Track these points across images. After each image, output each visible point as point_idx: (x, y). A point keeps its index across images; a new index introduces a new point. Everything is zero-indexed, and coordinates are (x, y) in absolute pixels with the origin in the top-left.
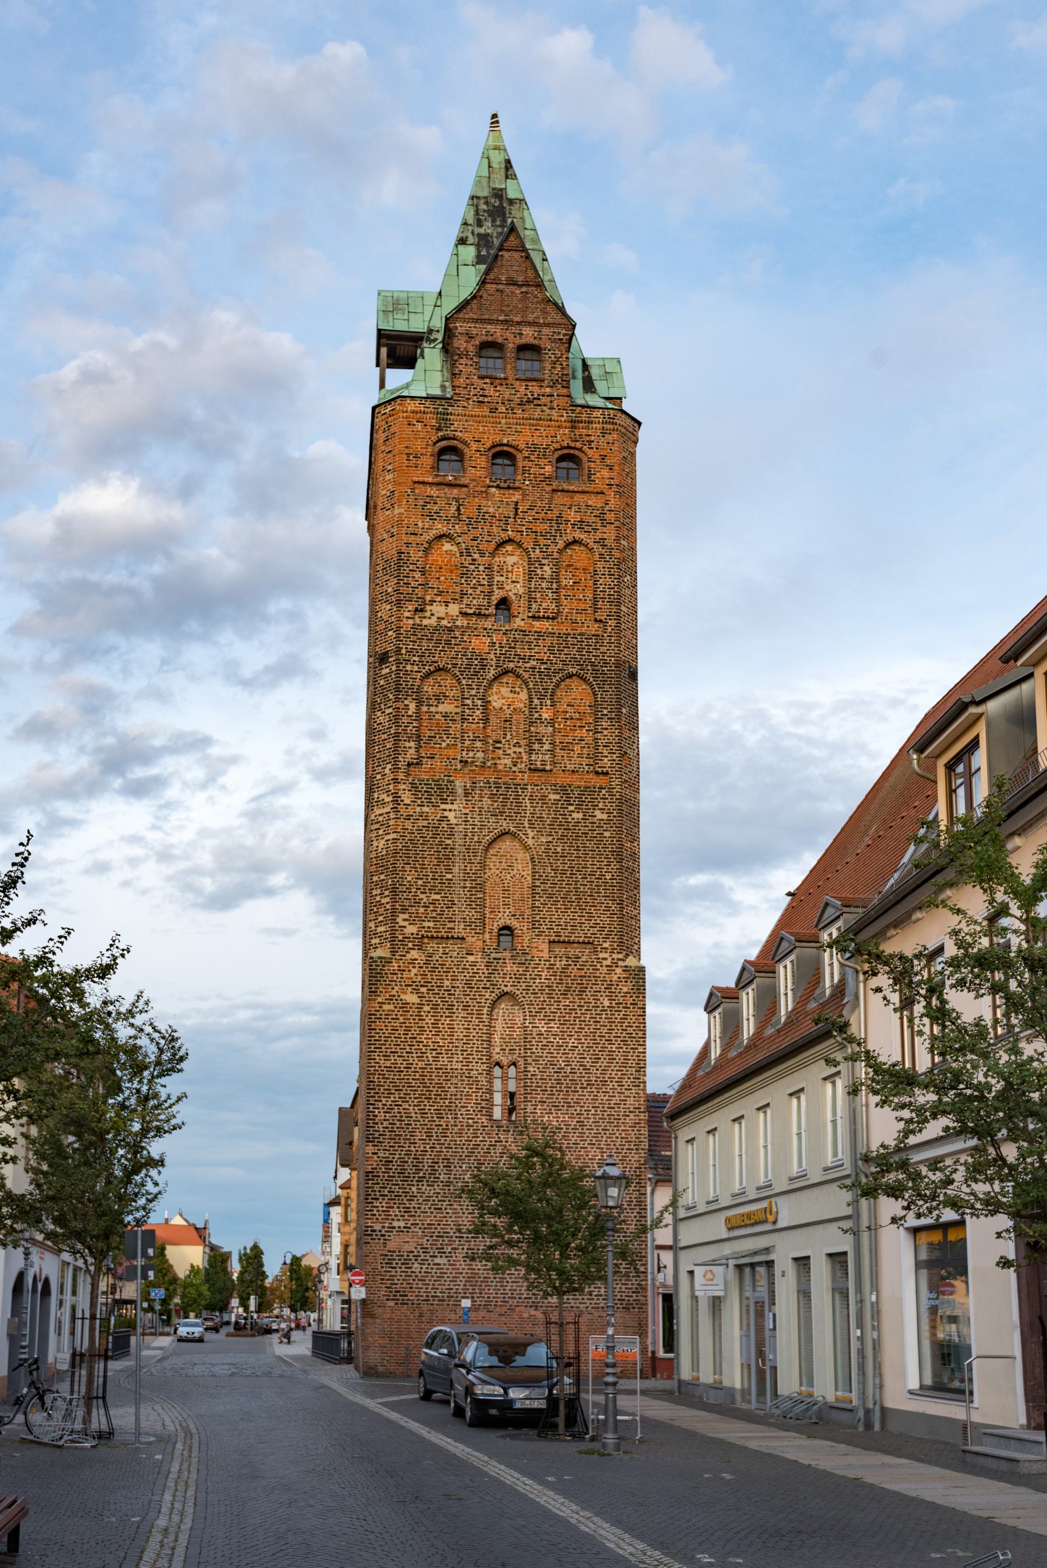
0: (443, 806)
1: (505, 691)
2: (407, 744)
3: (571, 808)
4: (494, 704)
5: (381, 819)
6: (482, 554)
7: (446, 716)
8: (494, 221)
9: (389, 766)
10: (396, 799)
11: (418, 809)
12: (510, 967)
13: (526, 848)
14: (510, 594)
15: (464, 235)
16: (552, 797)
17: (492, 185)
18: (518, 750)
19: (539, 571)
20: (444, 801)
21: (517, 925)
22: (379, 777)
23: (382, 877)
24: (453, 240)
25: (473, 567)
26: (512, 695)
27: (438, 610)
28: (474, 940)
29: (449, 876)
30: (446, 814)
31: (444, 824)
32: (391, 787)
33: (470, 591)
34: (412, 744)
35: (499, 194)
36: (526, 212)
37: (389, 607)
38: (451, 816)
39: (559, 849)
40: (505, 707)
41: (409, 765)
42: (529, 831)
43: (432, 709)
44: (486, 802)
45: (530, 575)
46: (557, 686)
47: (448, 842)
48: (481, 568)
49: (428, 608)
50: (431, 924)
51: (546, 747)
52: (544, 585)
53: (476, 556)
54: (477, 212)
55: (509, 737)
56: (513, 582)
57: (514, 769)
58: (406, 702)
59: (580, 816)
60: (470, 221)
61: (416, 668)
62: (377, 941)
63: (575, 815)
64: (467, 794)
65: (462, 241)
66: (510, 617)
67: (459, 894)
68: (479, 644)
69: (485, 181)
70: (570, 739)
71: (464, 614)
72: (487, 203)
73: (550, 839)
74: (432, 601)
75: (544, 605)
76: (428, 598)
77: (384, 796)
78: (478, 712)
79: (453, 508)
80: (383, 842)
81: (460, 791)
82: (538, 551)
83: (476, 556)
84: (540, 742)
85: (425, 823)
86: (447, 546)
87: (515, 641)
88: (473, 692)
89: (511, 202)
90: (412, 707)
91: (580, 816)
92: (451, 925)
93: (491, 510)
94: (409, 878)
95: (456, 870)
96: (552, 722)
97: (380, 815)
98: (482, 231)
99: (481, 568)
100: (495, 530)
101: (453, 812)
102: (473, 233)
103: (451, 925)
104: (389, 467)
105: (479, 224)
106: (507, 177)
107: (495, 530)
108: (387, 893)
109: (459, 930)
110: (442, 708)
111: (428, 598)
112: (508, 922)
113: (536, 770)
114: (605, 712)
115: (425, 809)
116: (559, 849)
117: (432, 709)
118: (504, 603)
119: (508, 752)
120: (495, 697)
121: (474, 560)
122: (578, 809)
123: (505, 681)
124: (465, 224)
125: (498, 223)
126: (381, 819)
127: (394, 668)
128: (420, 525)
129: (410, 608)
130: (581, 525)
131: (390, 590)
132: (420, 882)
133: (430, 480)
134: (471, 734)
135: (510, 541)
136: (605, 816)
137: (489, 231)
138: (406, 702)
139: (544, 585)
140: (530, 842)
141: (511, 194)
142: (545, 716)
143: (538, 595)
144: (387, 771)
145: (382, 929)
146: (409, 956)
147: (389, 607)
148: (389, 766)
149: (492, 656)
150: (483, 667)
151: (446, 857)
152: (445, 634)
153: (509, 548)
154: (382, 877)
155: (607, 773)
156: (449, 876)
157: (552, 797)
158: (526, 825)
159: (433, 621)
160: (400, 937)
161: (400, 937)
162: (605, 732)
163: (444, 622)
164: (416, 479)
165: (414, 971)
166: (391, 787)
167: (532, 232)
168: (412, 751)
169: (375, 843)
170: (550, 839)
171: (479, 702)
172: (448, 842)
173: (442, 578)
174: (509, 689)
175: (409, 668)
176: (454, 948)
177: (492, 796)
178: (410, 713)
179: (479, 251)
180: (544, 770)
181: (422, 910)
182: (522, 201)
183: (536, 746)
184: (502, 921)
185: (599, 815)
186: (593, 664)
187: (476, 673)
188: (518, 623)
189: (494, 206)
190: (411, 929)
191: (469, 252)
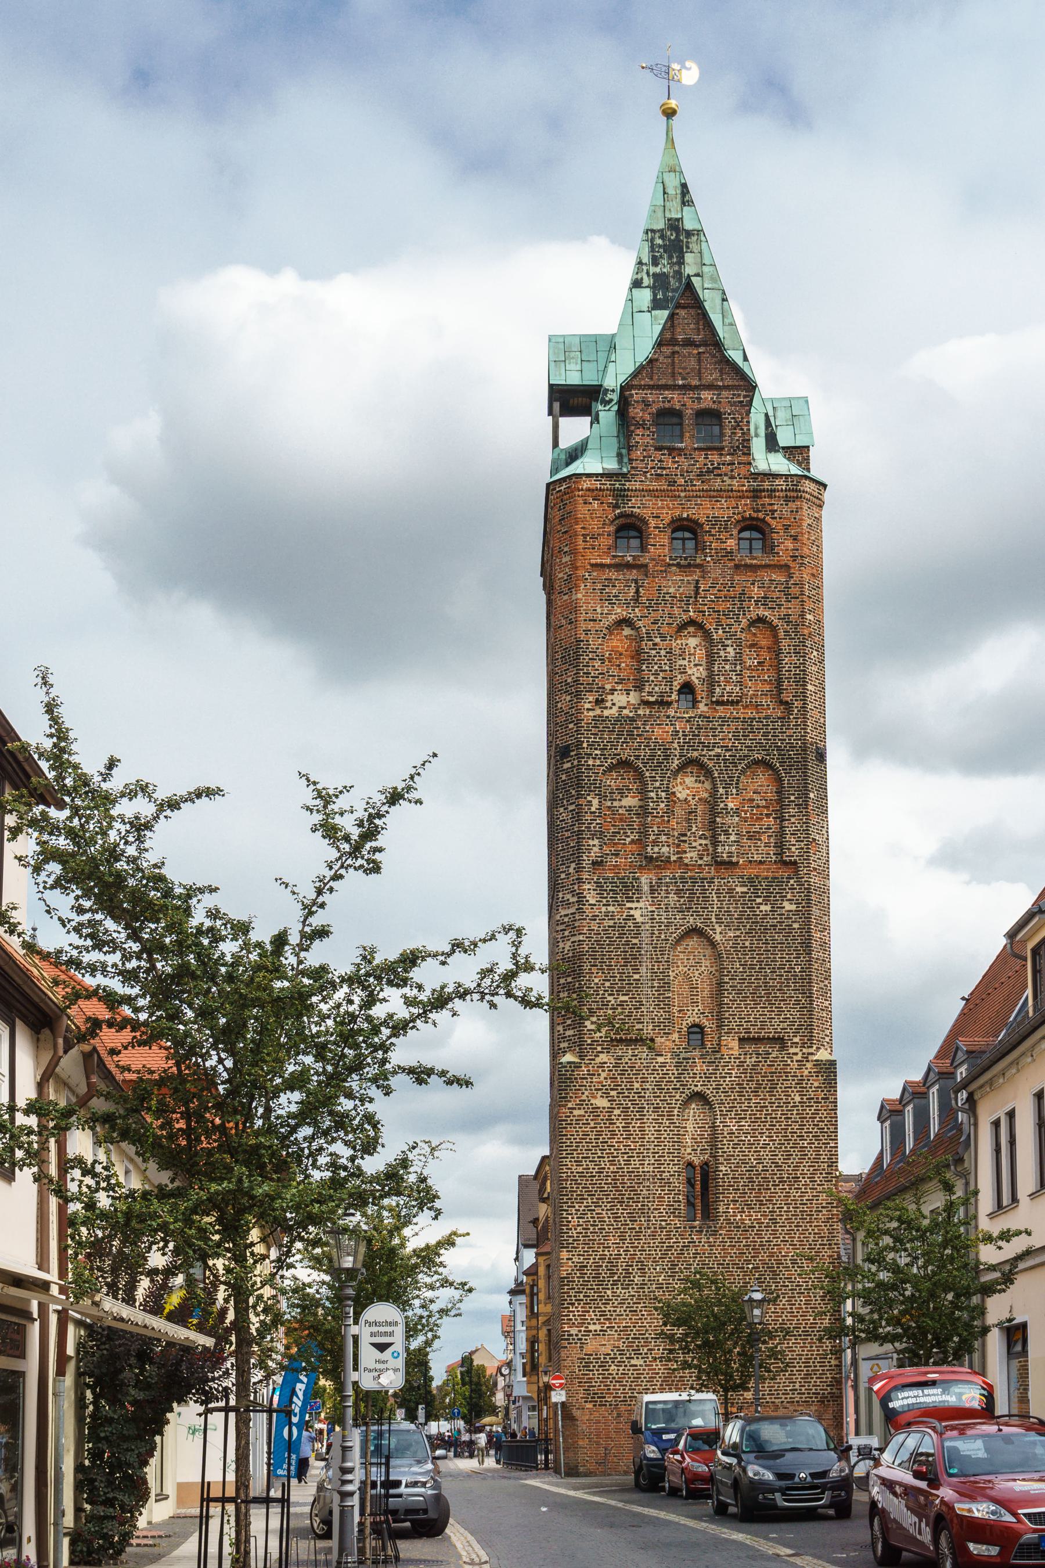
0: (629, 905)
1: (689, 781)
2: (591, 842)
3: (759, 900)
4: (678, 795)
5: (566, 919)
6: (663, 638)
7: (629, 809)
8: (670, 257)
9: (573, 865)
10: (581, 899)
11: (604, 909)
12: (700, 1067)
13: (713, 944)
14: (693, 678)
15: (639, 276)
16: (739, 889)
17: (668, 215)
18: (704, 842)
19: (722, 653)
20: (630, 900)
21: (707, 1023)
22: (563, 876)
23: (569, 979)
24: (627, 283)
25: (654, 652)
26: (697, 785)
27: (620, 699)
28: (663, 1040)
29: (636, 977)
30: (632, 912)
32: (576, 887)
33: (652, 678)
34: (596, 842)
35: (675, 225)
36: (704, 244)
37: (568, 698)
38: (637, 914)
39: (747, 944)
40: (690, 798)
41: (594, 863)
42: (716, 926)
43: (615, 804)
45: (711, 658)
46: (743, 772)
47: (635, 941)
48: (663, 653)
49: (610, 697)
51: (733, 838)
52: (727, 667)
53: (658, 640)
54: (652, 248)
55: (694, 829)
56: (696, 665)
57: (700, 862)
58: (589, 798)
59: (768, 908)
60: (645, 260)
61: (598, 762)
62: (566, 1045)
63: (763, 908)
64: (652, 891)
65: (637, 284)
66: (695, 703)
67: (648, 993)
68: (660, 733)
69: (660, 214)
71: (647, 703)
72: (662, 237)
73: (738, 933)
74: (613, 691)
75: (728, 688)
76: (608, 687)
77: (569, 896)
78: (662, 805)
79: (633, 590)
80: (569, 943)
81: (646, 888)
82: (720, 632)
83: (658, 640)
84: (727, 833)
85: (611, 923)
86: (627, 631)
87: (699, 728)
88: (657, 784)
89: (689, 234)
90: (595, 802)
91: (768, 908)
92: (640, 1026)
93: (672, 590)
94: (596, 980)
96: (737, 812)
97: (566, 915)
98: (657, 270)
99: (663, 653)
100: (676, 611)
101: (639, 910)
102: (648, 273)
103: (640, 1026)
104: (566, 549)
105: (655, 262)
106: (683, 203)
107: (676, 611)
108: (574, 996)
109: (648, 1030)
111: (608, 687)
112: (697, 1020)
113: (723, 863)
114: (792, 798)
115: (611, 908)
116: (747, 944)
117: (615, 804)
118: (687, 688)
119: (694, 844)
120: (680, 788)
121: (655, 644)
122: (766, 901)
123: (689, 770)
124: (640, 263)
125: (675, 260)
126: (566, 919)
127: (576, 763)
128: (599, 610)
129: (591, 699)
130: (764, 601)
131: (569, 680)
132: (607, 984)
133: (608, 561)
134: (655, 829)
135: (692, 622)
136: (793, 907)
137: (665, 270)
138: (589, 798)
139: (727, 667)
140: (718, 937)
141: (689, 225)
142: (731, 805)
143: (722, 678)
144: (571, 870)
145: (569, 1033)
146: (598, 1060)
147: (568, 698)
148: (573, 865)
149: (676, 745)
150: (667, 757)
151: (633, 958)
152: (625, 725)
153: (691, 629)
154: (569, 979)
155: (795, 863)
156: (636, 977)
157: (739, 889)
158: (714, 920)
159: (614, 711)
160: (589, 1041)
161: (589, 1041)
162: (793, 820)
163: (626, 712)
164: (593, 561)
165: (603, 1075)
166: (576, 887)
167: (712, 268)
168: (596, 849)
169: (561, 945)
170: (738, 933)
171: (663, 794)
172: (635, 941)
173: (623, 665)
174: (693, 779)
175: (590, 762)
176: (643, 1052)
177: (678, 892)
178: (593, 809)
179: (655, 295)
180: (730, 863)
181: (610, 1012)
182: (699, 232)
183: (722, 838)
184: (691, 1019)
185: (788, 906)
186: (779, 749)
188: (702, 707)
189: (670, 239)
191: (645, 296)
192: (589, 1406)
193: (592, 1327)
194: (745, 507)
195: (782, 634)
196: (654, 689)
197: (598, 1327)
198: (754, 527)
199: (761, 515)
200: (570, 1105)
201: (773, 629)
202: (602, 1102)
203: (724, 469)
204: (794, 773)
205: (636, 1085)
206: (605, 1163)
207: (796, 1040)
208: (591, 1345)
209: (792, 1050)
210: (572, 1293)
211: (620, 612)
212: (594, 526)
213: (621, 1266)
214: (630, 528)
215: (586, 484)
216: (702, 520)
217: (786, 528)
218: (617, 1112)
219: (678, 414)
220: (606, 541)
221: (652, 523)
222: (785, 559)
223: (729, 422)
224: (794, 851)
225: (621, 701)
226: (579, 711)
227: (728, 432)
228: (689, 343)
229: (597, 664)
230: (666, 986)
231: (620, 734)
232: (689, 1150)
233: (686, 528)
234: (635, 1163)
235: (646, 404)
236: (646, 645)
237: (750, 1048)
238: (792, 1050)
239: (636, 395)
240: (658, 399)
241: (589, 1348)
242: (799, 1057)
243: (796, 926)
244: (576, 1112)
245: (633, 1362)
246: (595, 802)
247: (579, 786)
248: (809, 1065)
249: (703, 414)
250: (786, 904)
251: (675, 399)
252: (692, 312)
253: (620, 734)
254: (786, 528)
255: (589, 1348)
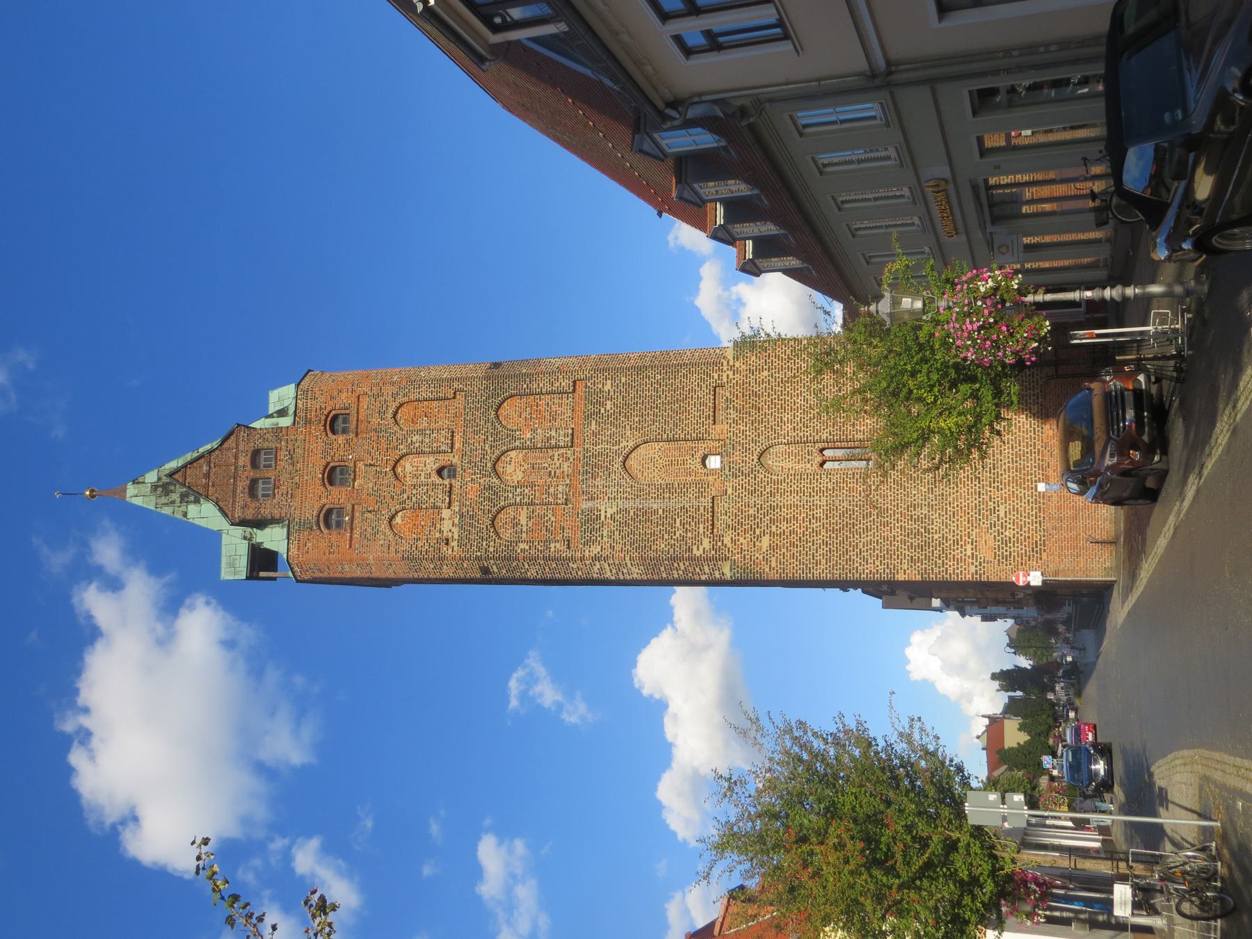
1: (510, 469)
3: (603, 410)
6: (404, 491)
7: (530, 518)
10: (596, 558)
20: (599, 517)
27: (446, 526)
29: (660, 512)
31: (617, 517)
38: (610, 511)
44: (598, 482)
45: (420, 453)
50: (701, 526)
51: (553, 433)
59: (609, 403)
62: (717, 573)
63: (608, 407)
64: (592, 499)
67: (675, 503)
68: (473, 492)
70: (547, 415)
71: (450, 503)
74: (441, 531)
76: (438, 535)
77: (596, 569)
81: (590, 504)
83: (405, 496)
84: (549, 438)
85: (617, 533)
86: (398, 520)
87: (470, 462)
90: (522, 546)
91: (609, 403)
95: (655, 506)
96: (534, 431)
101: (607, 509)
109: (706, 502)
110: (523, 521)
111: (438, 535)
115: (605, 533)
122: (604, 405)
130: (382, 413)
132: (666, 536)
135: (394, 469)
136: (609, 382)
140: (631, 444)
142: (529, 436)
145: (706, 568)
146: (729, 545)
150: (490, 488)
151: (645, 515)
152: (465, 520)
153: (399, 470)
155: (574, 382)
156: (660, 512)
157: (593, 427)
159: (455, 530)
163: (456, 521)
165: (742, 540)
168: (558, 545)
175: (491, 549)
176: (722, 506)
177: (594, 477)
181: (689, 534)
183: (553, 442)
187: (495, 493)
188: (456, 460)
190: (706, 544)
192: (1044, 556)
193: (969, 553)
194: (317, 430)
195: (406, 399)
196: (440, 497)
197: (969, 547)
198: (334, 423)
199: (323, 418)
200: (767, 570)
201: (401, 405)
202: (765, 542)
203: (290, 447)
204: (506, 386)
205: (751, 512)
206: (818, 539)
207: (716, 377)
208: (986, 554)
209: (725, 379)
210: (936, 570)
211: (384, 526)
212: (323, 545)
213: (912, 525)
214: (329, 518)
215: (294, 552)
216: (324, 462)
217: (332, 398)
218: (774, 529)
219: (254, 483)
220: (334, 535)
221: (324, 501)
222: (354, 399)
223: (260, 443)
224: (565, 384)
225: (448, 524)
226: (454, 558)
227: (266, 445)
228: (207, 475)
229: (420, 544)
230: (669, 487)
231: (471, 525)
232: (809, 466)
233: (332, 475)
234: (819, 513)
235: (245, 506)
236: (409, 504)
237: (721, 415)
238: (725, 379)
239: (238, 514)
240: (242, 497)
241: (990, 557)
242: (731, 373)
243: (623, 380)
244: (773, 565)
245: (1002, 514)
246: (522, 546)
247: (509, 559)
248: (737, 364)
249: (254, 464)
250: (606, 389)
251: (243, 484)
252: (189, 472)
253: (471, 525)
254: (332, 398)
255: (990, 557)
